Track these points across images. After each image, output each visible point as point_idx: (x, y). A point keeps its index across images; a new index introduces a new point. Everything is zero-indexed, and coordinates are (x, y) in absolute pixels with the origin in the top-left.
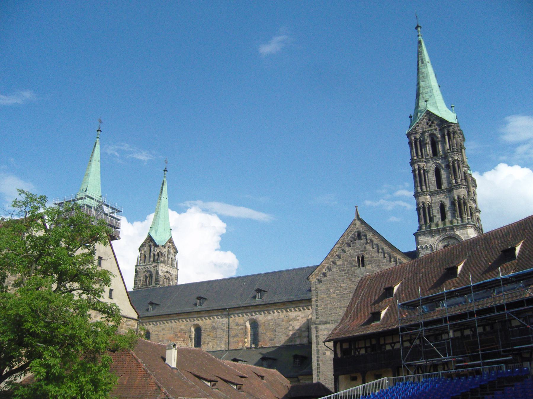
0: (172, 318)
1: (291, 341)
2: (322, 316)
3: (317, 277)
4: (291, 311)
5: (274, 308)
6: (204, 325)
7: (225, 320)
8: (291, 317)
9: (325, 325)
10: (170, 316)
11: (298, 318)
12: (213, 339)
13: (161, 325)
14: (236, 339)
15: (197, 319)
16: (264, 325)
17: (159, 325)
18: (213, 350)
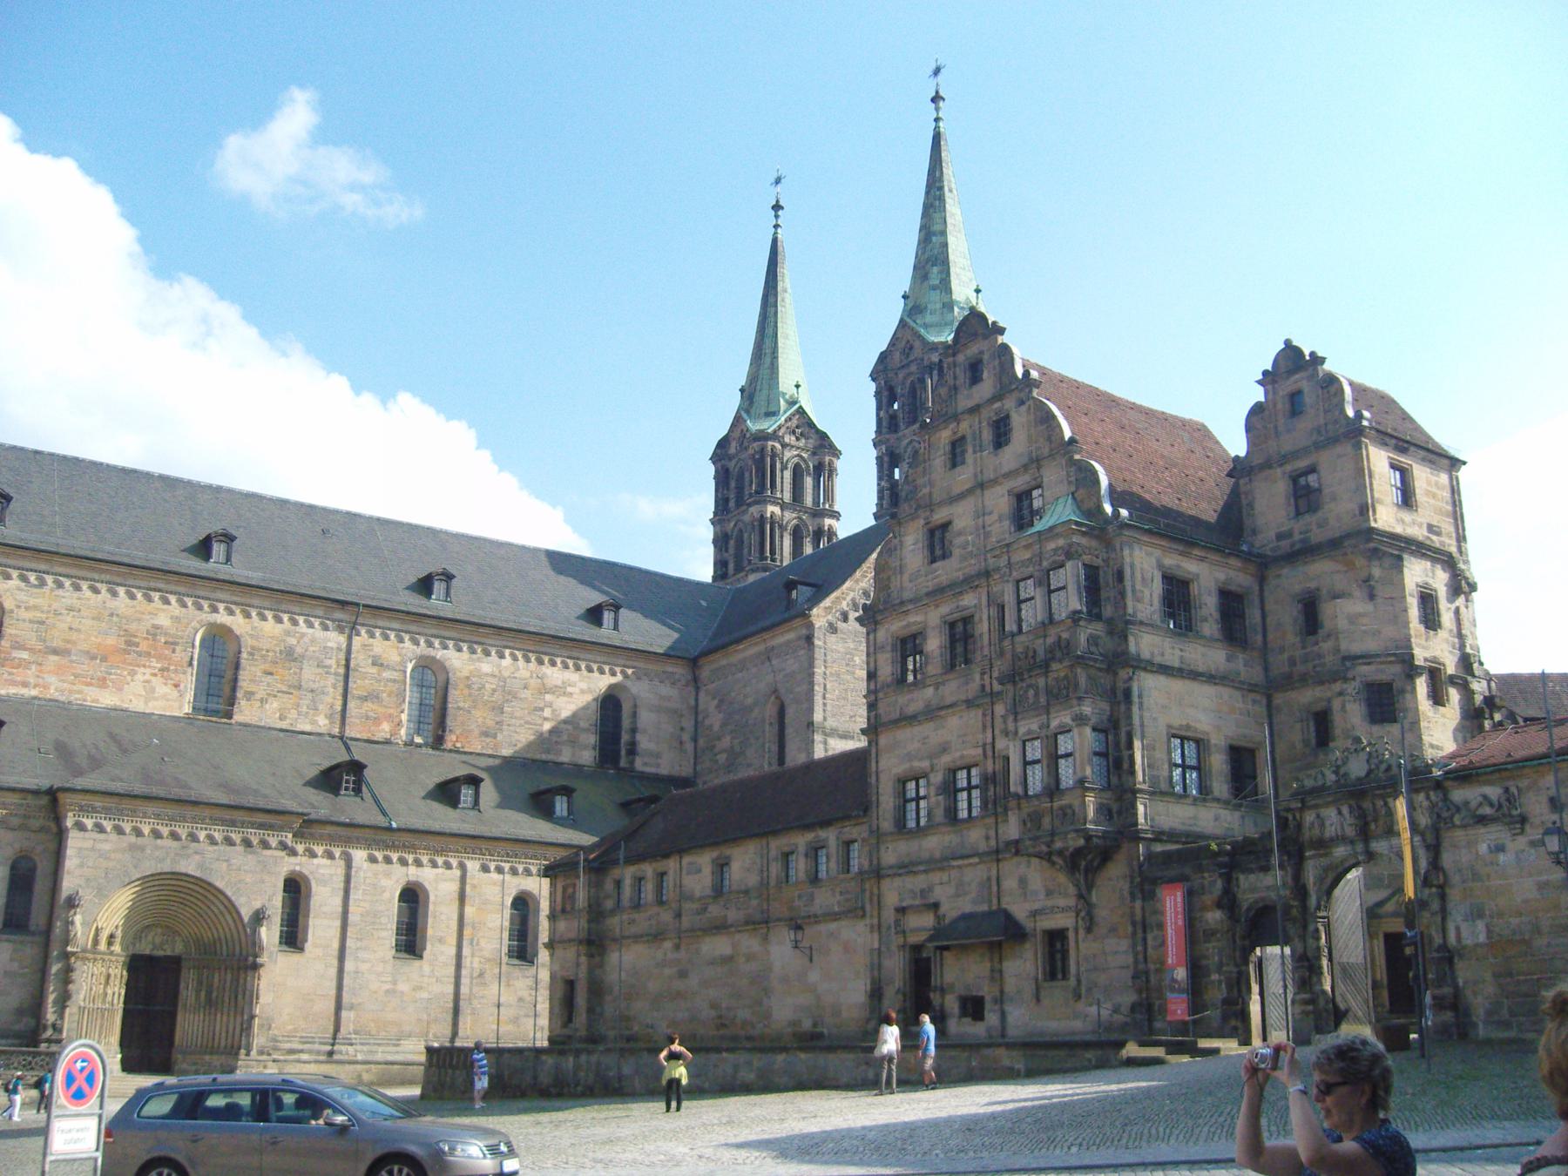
0: (118, 580)
1: (548, 751)
2: (834, 716)
3: (830, 617)
4: (553, 664)
5: (505, 643)
6: (252, 636)
7: (336, 639)
8: (550, 682)
9: (844, 741)
10: (115, 568)
11: (569, 689)
12: (284, 689)
13: (60, 592)
14: (368, 706)
15: (227, 609)
16: (469, 687)
17: (52, 590)
18: (284, 727)
